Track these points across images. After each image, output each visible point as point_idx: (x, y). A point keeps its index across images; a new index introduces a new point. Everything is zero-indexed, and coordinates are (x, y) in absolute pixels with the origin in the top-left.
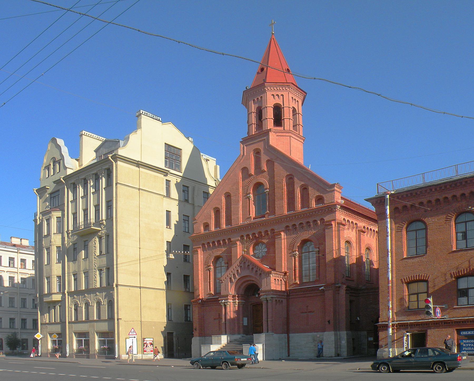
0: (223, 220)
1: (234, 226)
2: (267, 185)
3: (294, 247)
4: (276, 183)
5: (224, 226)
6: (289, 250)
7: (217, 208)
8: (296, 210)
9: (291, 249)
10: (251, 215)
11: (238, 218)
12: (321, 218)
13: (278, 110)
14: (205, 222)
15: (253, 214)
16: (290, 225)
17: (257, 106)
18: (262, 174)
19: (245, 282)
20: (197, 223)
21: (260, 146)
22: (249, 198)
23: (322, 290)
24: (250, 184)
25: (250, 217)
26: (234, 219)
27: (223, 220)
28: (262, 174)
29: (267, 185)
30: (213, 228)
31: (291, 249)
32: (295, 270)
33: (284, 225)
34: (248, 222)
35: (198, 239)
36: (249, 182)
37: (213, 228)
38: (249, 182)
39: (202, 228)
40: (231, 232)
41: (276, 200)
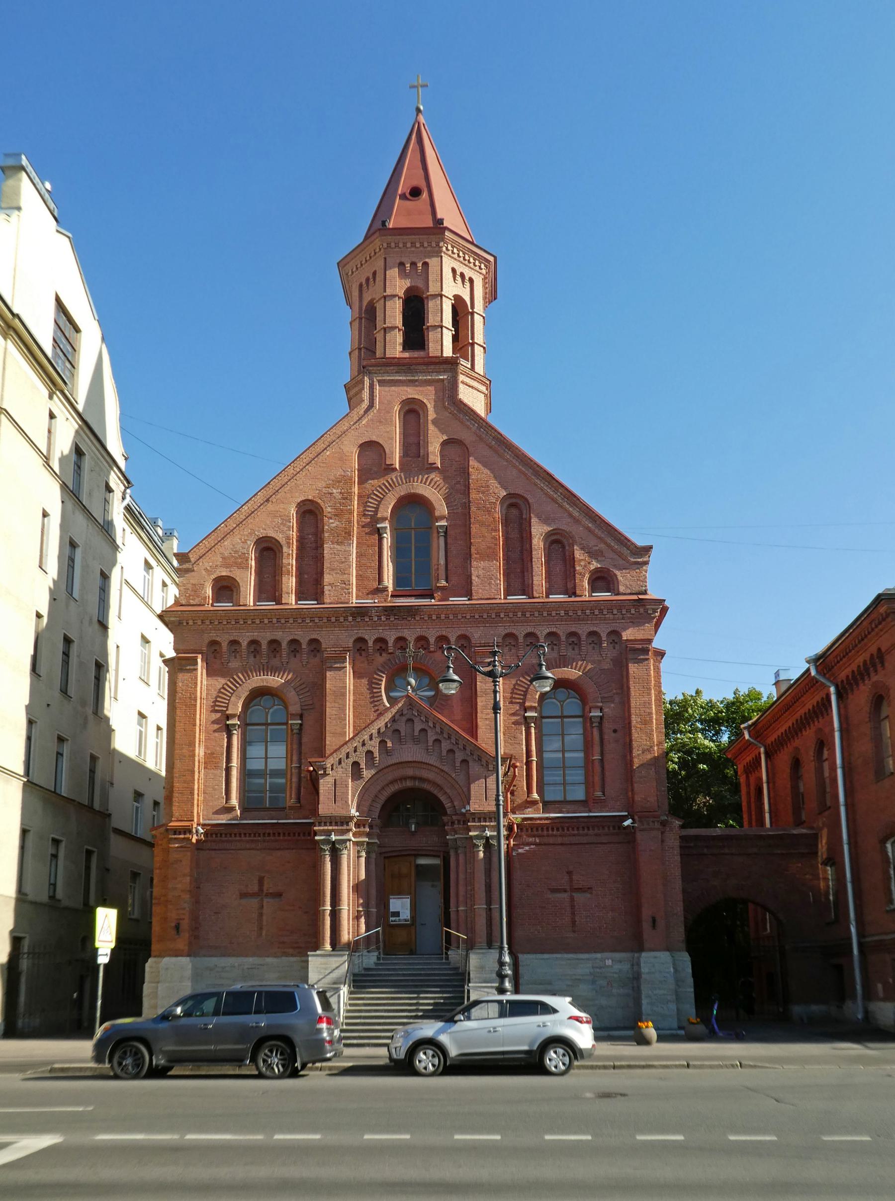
0: (290, 583)
1: (330, 603)
2: (442, 509)
3: (529, 696)
4: (473, 509)
5: (291, 600)
6: (511, 703)
7: (266, 541)
8: (536, 594)
9: (518, 701)
10: (386, 583)
11: (346, 583)
12: (610, 630)
13: (461, 312)
14: (224, 574)
15: (389, 581)
16: (521, 631)
17: (407, 283)
18: (426, 476)
19: (404, 778)
20: (193, 571)
21: (427, 396)
22: (379, 533)
23: (628, 826)
24: (387, 493)
25: (385, 589)
26: (330, 584)
27: (290, 583)
28: (426, 476)
29: (442, 509)
30: (249, 597)
31: (518, 701)
32: (528, 763)
33: (502, 631)
34: (376, 601)
35: (199, 622)
36: (383, 487)
37: (249, 597)
38: (383, 487)
39: (209, 592)
40: (325, 620)
41: (474, 556)
